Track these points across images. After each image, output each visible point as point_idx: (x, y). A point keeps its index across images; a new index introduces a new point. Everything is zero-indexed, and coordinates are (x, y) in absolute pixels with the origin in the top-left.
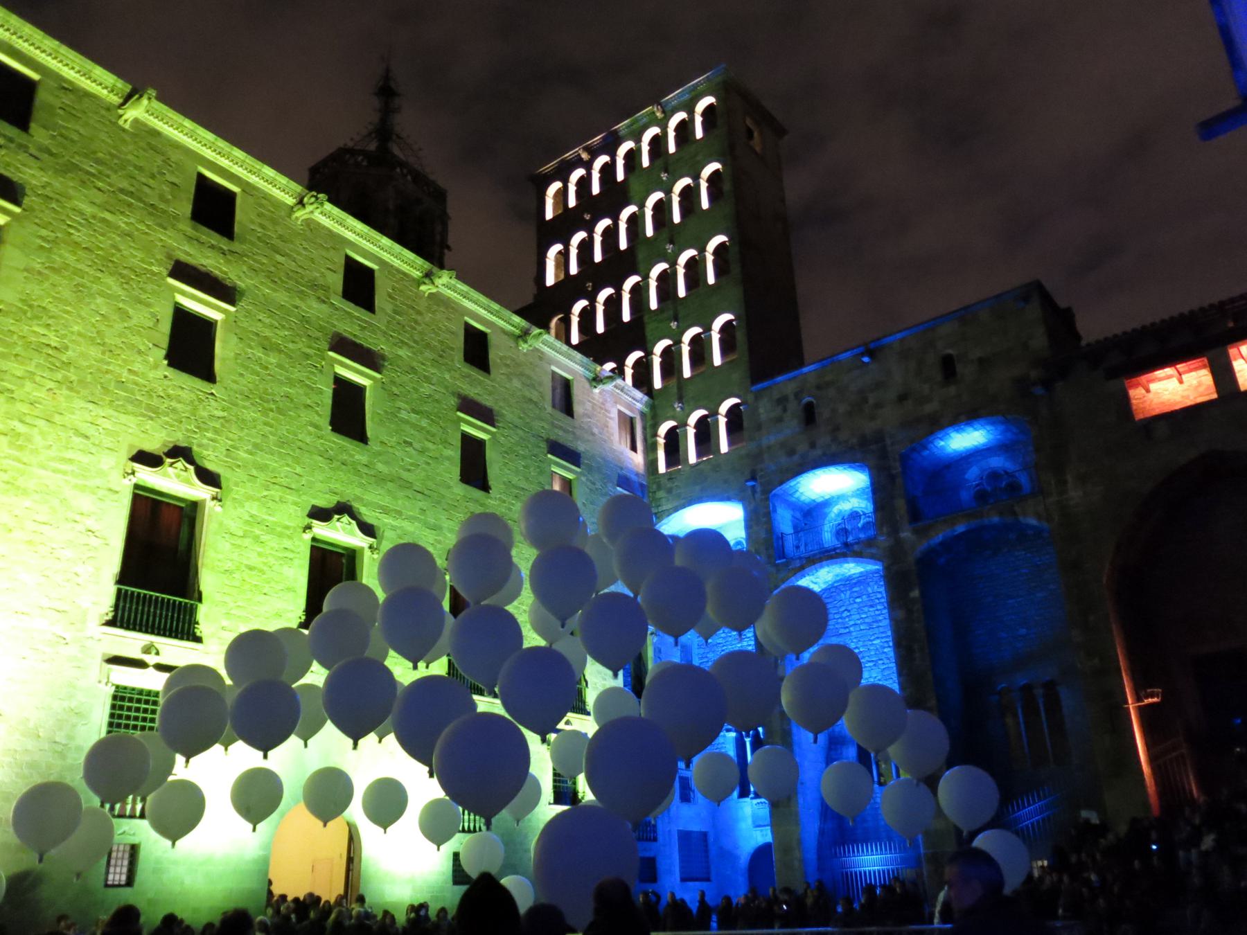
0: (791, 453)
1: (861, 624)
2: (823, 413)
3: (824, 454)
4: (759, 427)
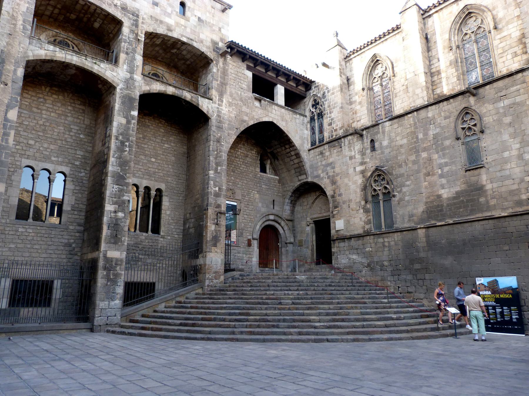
1: (53, 112)
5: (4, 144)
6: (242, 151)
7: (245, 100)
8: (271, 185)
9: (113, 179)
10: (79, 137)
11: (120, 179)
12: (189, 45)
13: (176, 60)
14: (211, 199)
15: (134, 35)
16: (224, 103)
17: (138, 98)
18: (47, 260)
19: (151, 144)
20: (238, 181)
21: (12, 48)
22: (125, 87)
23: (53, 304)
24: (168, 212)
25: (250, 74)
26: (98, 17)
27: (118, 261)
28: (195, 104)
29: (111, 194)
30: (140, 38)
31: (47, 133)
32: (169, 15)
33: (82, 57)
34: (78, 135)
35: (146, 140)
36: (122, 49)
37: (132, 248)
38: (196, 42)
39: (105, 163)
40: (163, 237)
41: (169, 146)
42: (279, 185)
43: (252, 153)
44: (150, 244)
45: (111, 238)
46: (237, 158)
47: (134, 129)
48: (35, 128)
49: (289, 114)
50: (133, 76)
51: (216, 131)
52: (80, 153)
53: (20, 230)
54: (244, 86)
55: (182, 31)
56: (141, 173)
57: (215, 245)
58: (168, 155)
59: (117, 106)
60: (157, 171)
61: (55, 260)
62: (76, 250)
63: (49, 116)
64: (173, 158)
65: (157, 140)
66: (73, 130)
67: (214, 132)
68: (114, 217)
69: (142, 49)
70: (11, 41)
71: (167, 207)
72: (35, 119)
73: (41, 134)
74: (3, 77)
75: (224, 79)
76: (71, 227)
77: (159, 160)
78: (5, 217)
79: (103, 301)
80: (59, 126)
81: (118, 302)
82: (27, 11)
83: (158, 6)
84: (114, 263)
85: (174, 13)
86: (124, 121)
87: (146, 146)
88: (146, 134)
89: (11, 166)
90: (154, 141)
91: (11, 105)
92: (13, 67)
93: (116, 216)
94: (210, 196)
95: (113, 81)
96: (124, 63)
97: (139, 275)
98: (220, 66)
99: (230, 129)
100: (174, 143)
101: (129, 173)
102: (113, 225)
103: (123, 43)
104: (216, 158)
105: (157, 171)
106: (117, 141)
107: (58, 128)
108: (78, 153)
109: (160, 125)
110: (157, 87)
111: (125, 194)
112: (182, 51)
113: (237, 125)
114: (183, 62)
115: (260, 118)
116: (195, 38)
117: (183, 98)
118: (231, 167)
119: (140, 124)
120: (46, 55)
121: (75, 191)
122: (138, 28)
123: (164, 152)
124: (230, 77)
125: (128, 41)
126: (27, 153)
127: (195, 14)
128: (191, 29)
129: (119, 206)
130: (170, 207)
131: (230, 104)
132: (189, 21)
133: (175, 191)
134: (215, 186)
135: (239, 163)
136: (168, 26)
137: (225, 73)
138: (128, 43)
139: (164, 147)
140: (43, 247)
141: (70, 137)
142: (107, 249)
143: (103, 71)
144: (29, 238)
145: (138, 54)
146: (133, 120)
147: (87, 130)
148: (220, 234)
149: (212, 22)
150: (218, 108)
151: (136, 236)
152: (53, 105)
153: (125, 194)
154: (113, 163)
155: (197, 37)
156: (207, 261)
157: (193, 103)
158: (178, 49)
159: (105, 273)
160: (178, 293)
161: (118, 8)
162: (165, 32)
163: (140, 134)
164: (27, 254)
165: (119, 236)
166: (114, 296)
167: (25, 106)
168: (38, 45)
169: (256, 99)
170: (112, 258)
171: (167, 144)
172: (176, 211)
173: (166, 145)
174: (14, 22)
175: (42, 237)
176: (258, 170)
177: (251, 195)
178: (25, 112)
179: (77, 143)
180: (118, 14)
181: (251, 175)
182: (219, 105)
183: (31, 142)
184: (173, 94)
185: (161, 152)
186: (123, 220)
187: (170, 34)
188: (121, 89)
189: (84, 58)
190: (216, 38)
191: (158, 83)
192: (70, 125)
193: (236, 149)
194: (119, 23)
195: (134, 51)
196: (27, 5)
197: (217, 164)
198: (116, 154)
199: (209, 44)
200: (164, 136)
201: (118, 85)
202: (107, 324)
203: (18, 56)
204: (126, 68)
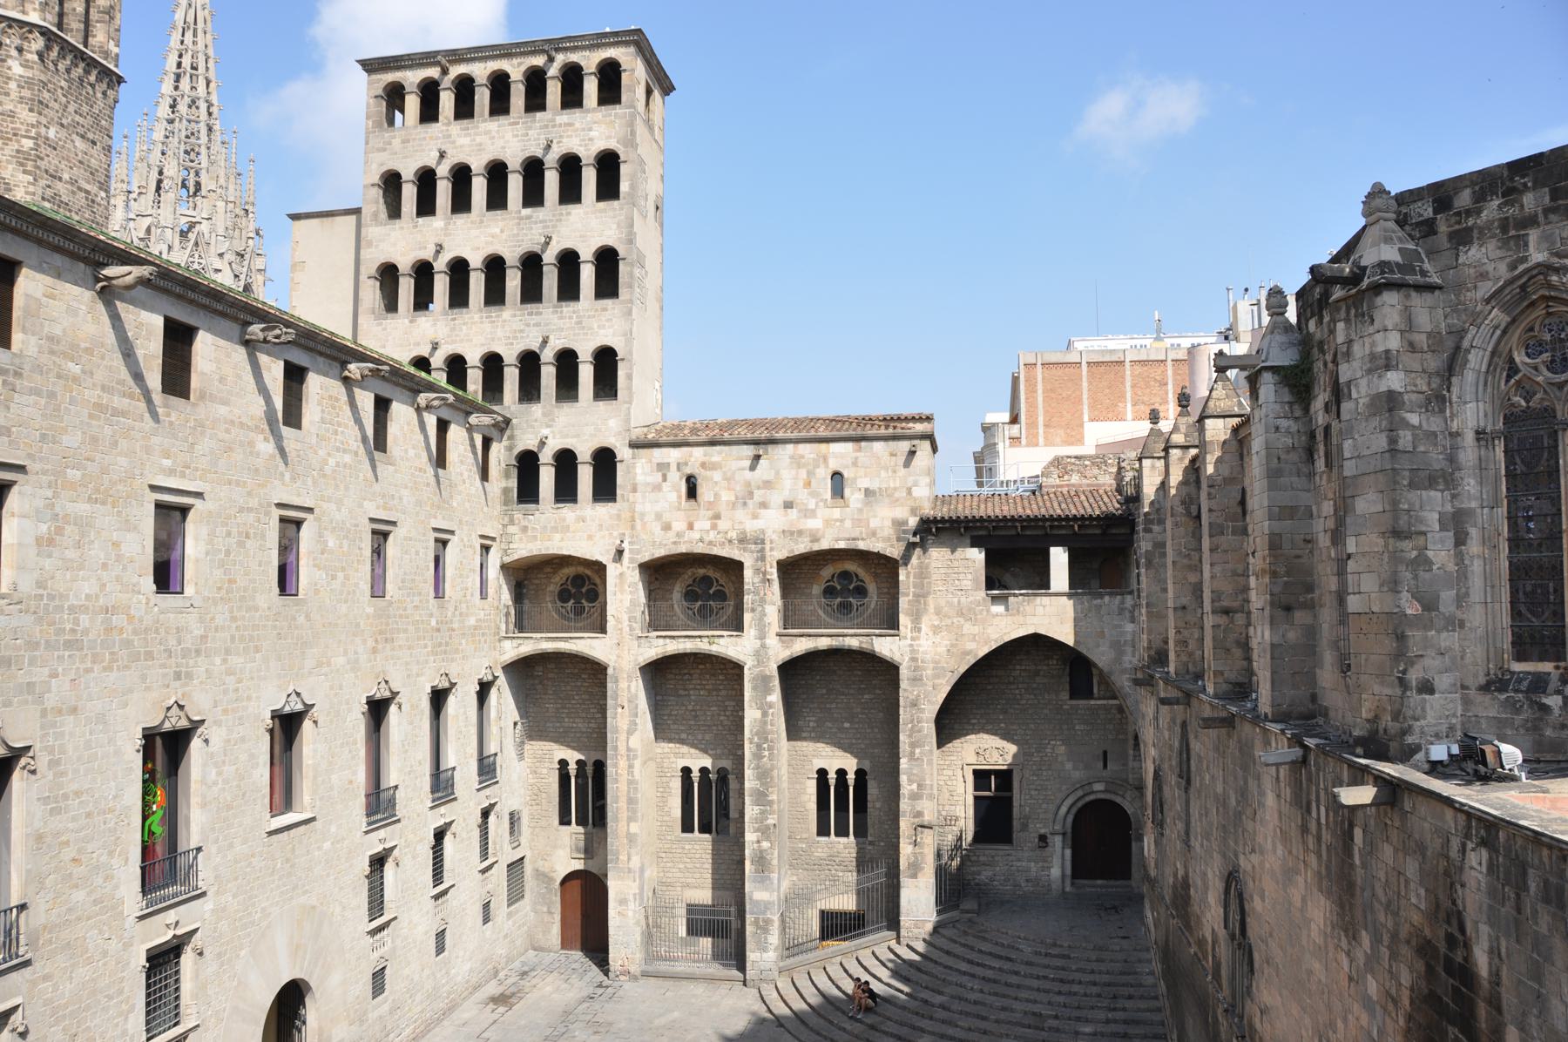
0: (667, 527)
3: (701, 540)
4: (634, 490)
6: (1023, 668)
7: (970, 609)
8: (1099, 721)
14: (904, 805)
17: (775, 673)
20: (1014, 727)
24: (878, 805)
25: (977, 556)
30: (768, 577)
32: (811, 514)
38: (863, 539)
40: (871, 843)
41: (872, 696)
42: (1119, 716)
43: (1048, 665)
46: (1014, 683)
49: (1083, 603)
51: (908, 688)
53: (687, 847)
54: (967, 583)
57: (914, 876)
60: (854, 741)
61: (728, 882)
64: (881, 714)
67: (905, 690)
71: (875, 797)
73: (692, 722)
83: (792, 508)
85: (821, 504)
86: (758, 714)
87: (834, 706)
96: (750, 627)
97: (841, 901)
99: (936, 676)
100: (880, 689)
103: (746, 597)
104: (910, 736)
105: (854, 741)
109: (853, 664)
110: (801, 646)
113: (952, 664)
115: (1005, 634)
118: (999, 704)
124: (934, 577)
131: (936, 630)
135: (1017, 692)
137: (923, 574)
144: (698, 856)
148: (922, 858)
149: (892, 485)
150: (911, 645)
160: (860, 944)
164: (698, 875)
168: (647, 645)
169: (995, 599)
173: (866, 696)
174: (620, 626)
176: (1065, 695)
177: (1048, 750)
181: (1046, 711)
182: (913, 639)
183: (684, 736)
185: (859, 710)
187: (816, 547)
188: (750, 669)
190: (901, 512)
192: (723, 702)
193: (1010, 667)
195: (763, 601)
197: (913, 745)
199: (888, 531)
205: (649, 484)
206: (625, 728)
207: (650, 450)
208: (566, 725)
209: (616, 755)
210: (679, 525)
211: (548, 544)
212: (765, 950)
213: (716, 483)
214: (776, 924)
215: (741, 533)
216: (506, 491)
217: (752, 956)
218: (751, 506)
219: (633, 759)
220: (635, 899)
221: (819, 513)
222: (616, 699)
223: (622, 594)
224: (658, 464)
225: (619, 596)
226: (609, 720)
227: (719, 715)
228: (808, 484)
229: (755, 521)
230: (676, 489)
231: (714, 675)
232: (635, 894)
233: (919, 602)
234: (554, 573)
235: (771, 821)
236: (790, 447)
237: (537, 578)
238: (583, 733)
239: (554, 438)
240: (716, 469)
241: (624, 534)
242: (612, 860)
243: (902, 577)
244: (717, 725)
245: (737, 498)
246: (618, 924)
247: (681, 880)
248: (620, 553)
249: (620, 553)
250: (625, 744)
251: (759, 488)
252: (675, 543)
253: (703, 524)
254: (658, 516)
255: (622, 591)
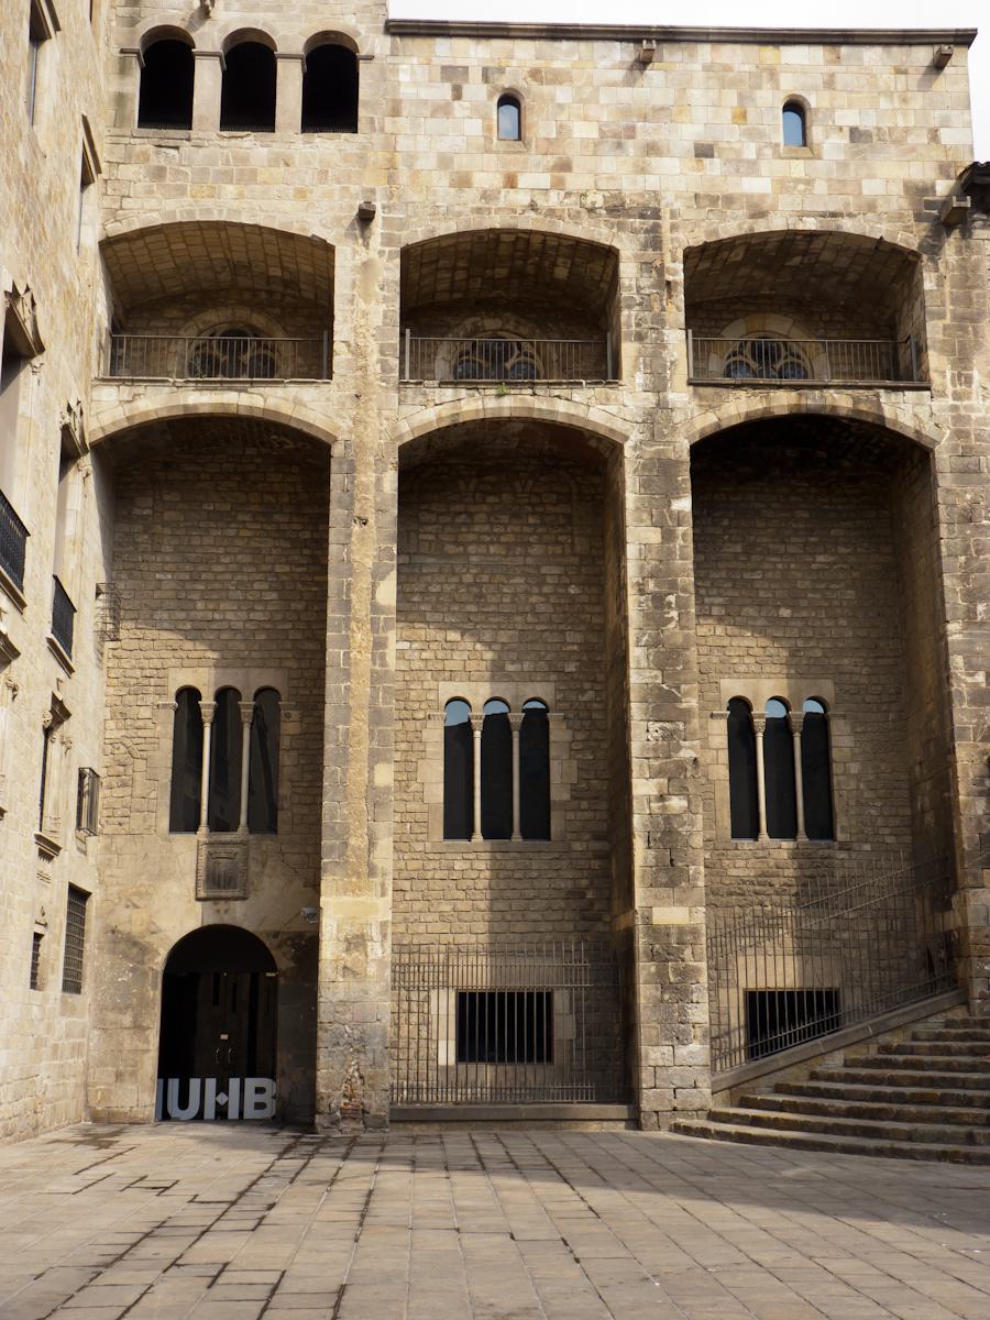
1: (492, 542)
2: (541, 127)
3: (533, 207)
5: (377, 668)
9: (644, 705)
10: (568, 594)
11: (664, 704)
12: (831, 233)
13: (813, 280)
15: (654, 272)
16: (974, 386)
17: (686, 457)
18: (529, 937)
19: (771, 566)
21: (366, 428)
22: (646, 435)
23: (557, 1056)
24: (854, 768)
26: (557, 255)
27: (685, 935)
28: (870, 420)
29: (644, 748)
30: (670, 278)
31: (487, 604)
32: (752, 168)
33: (524, 391)
34: (563, 590)
35: (754, 558)
36: (624, 329)
37: (751, 888)
38: (850, 215)
39: (623, 659)
40: (845, 847)
41: (832, 559)
44: (808, 873)
45: (659, 871)
47: (685, 550)
48: (456, 596)
50: (664, 397)
51: (954, 486)
52: (574, 638)
53: (458, 865)
55: (799, 200)
56: (752, 660)
58: (833, 586)
59: (631, 498)
60: (800, 644)
62: (596, 908)
63: (484, 555)
64: (851, 594)
65: (791, 549)
66: (549, 580)
67: (948, 491)
68: (657, 811)
69: (682, 306)
70: (362, 412)
72: (454, 574)
73: (473, 608)
74: (357, 505)
75: (968, 301)
76: (577, 846)
77: (805, 608)
78: (420, 837)
79: (657, 1045)
80: (514, 577)
81: (696, 1050)
82: (385, 324)
83: (712, 156)
84: (673, 940)
85: (768, 152)
86: (654, 536)
88: (752, 538)
89: (416, 706)
90: (781, 556)
91: (381, 570)
92: (374, 475)
93: (665, 808)
94: (956, 704)
95: (612, 430)
96: (636, 367)
98: (947, 262)
100: (846, 545)
101: (685, 683)
102: (659, 835)
103: (625, 313)
104: (965, 579)
105: (800, 644)
106: (642, 598)
107: (511, 581)
108: (568, 640)
109: (793, 498)
110: (738, 406)
111: (682, 743)
112: (820, 254)
114: (835, 280)
116: (847, 205)
117: (827, 412)
119: (732, 514)
120: (440, 419)
121: (574, 747)
122: (661, 250)
123: (818, 581)
125: (638, 300)
126: (449, 665)
127: (839, 123)
128: (829, 180)
129: (669, 780)
130: (857, 751)
132: (820, 158)
133: (868, 698)
134: (972, 668)
136: (750, 206)
137: (967, 279)
138: (640, 304)
139: (814, 566)
140: (515, 905)
141: (543, 599)
142: (651, 902)
143: (580, 411)
145: (671, 328)
146: (679, 525)
147: (583, 570)
149: (901, 124)
150: (955, 408)
151: (761, 853)
152: (491, 524)
153: (682, 743)
154: (638, 662)
155: (851, 198)
156: (970, 916)
157: (864, 418)
158: (805, 253)
159: (653, 969)
161: (601, 215)
162: (745, 227)
163: (735, 542)
165: (680, 864)
166: (684, 1030)
167: (427, 545)
168: (420, 399)
170: (667, 927)
171: (825, 553)
172: (883, 761)
173: (821, 558)
174: (361, 362)
175: (509, 878)
178: (430, 560)
179: (565, 612)
180: (601, 233)
182: (957, 396)
184: (794, 411)
186: (685, 819)
187: (761, 227)
188: (635, 448)
189: (530, 391)
190: (921, 172)
191: (742, 393)
192: (538, 568)
194: (610, 255)
195: (659, 323)
196: (384, 307)
198: (644, 634)
199: (899, 202)
200: (811, 532)
201: (626, 438)
202: (675, 1109)
203: (380, 444)
204: (641, 381)
205: (425, 102)
206: (369, 563)
207: (429, 41)
208: (200, 615)
209: (347, 621)
210: (487, 177)
211: (209, 203)
212: (681, 1039)
213: (561, 107)
214: (704, 979)
215: (612, 196)
216: (120, 99)
217: (653, 1054)
218: (631, 151)
219: (386, 629)
220: (384, 936)
221: (764, 166)
222: (349, 507)
223: (365, 301)
224: (444, 69)
225: (362, 305)
226: (333, 549)
227: (528, 593)
228: (741, 116)
229: (640, 178)
230: (477, 111)
231: (516, 515)
232: (383, 925)
233: (964, 329)
234: (187, 318)
235: (686, 754)
236: (705, 51)
237: (148, 328)
238: (237, 631)
239: (227, 8)
240: (561, 83)
241: (373, 191)
242: (332, 848)
243: (929, 284)
244: (524, 613)
245: (603, 134)
246: (341, 996)
247: (444, 939)
248: (365, 217)
249: (365, 217)
250: (366, 596)
251: (645, 119)
252: (479, 210)
253: (535, 178)
254: (444, 162)
255: (367, 298)
